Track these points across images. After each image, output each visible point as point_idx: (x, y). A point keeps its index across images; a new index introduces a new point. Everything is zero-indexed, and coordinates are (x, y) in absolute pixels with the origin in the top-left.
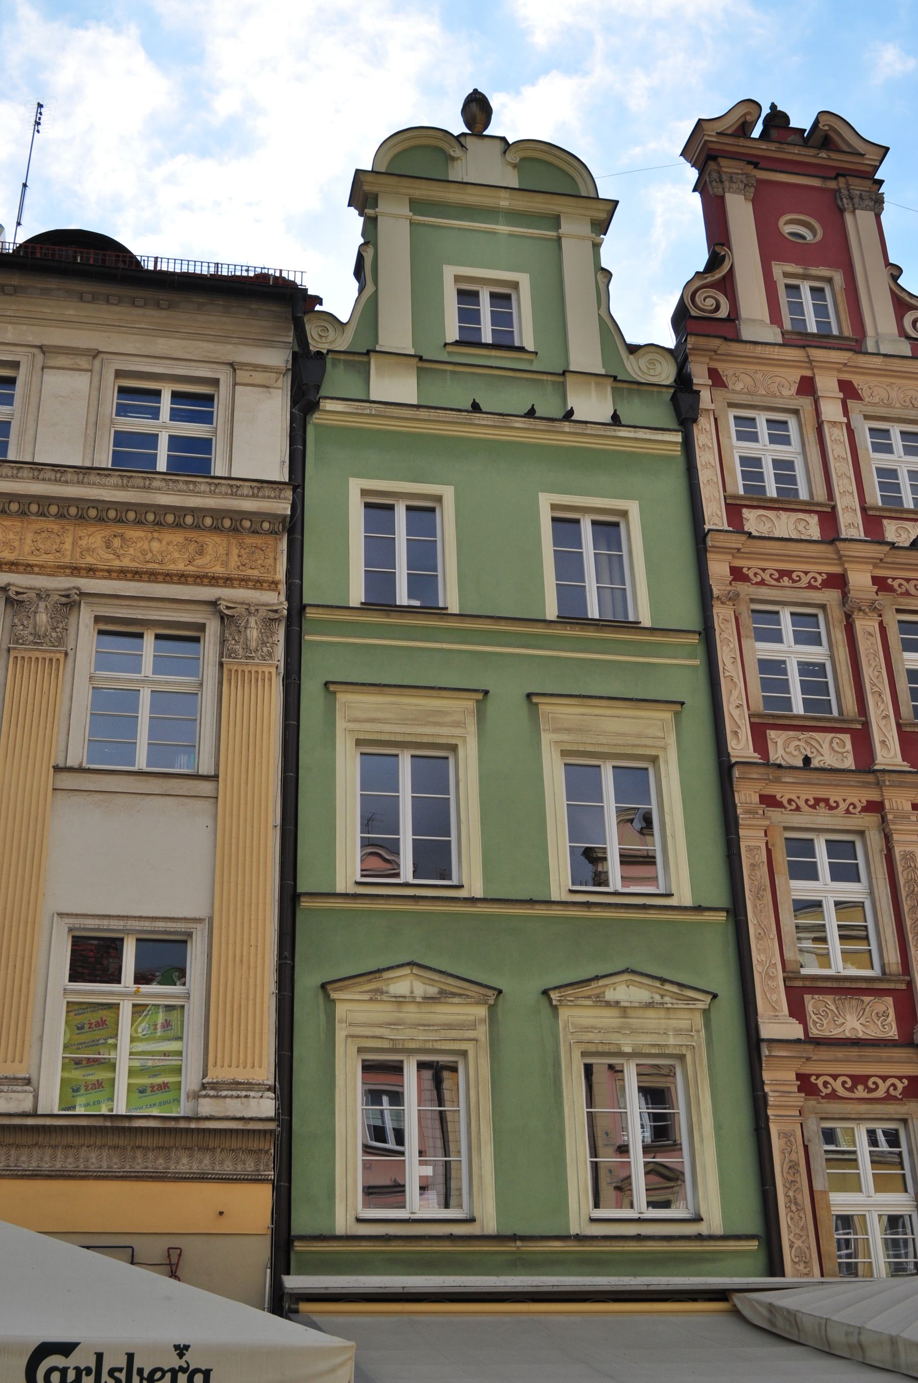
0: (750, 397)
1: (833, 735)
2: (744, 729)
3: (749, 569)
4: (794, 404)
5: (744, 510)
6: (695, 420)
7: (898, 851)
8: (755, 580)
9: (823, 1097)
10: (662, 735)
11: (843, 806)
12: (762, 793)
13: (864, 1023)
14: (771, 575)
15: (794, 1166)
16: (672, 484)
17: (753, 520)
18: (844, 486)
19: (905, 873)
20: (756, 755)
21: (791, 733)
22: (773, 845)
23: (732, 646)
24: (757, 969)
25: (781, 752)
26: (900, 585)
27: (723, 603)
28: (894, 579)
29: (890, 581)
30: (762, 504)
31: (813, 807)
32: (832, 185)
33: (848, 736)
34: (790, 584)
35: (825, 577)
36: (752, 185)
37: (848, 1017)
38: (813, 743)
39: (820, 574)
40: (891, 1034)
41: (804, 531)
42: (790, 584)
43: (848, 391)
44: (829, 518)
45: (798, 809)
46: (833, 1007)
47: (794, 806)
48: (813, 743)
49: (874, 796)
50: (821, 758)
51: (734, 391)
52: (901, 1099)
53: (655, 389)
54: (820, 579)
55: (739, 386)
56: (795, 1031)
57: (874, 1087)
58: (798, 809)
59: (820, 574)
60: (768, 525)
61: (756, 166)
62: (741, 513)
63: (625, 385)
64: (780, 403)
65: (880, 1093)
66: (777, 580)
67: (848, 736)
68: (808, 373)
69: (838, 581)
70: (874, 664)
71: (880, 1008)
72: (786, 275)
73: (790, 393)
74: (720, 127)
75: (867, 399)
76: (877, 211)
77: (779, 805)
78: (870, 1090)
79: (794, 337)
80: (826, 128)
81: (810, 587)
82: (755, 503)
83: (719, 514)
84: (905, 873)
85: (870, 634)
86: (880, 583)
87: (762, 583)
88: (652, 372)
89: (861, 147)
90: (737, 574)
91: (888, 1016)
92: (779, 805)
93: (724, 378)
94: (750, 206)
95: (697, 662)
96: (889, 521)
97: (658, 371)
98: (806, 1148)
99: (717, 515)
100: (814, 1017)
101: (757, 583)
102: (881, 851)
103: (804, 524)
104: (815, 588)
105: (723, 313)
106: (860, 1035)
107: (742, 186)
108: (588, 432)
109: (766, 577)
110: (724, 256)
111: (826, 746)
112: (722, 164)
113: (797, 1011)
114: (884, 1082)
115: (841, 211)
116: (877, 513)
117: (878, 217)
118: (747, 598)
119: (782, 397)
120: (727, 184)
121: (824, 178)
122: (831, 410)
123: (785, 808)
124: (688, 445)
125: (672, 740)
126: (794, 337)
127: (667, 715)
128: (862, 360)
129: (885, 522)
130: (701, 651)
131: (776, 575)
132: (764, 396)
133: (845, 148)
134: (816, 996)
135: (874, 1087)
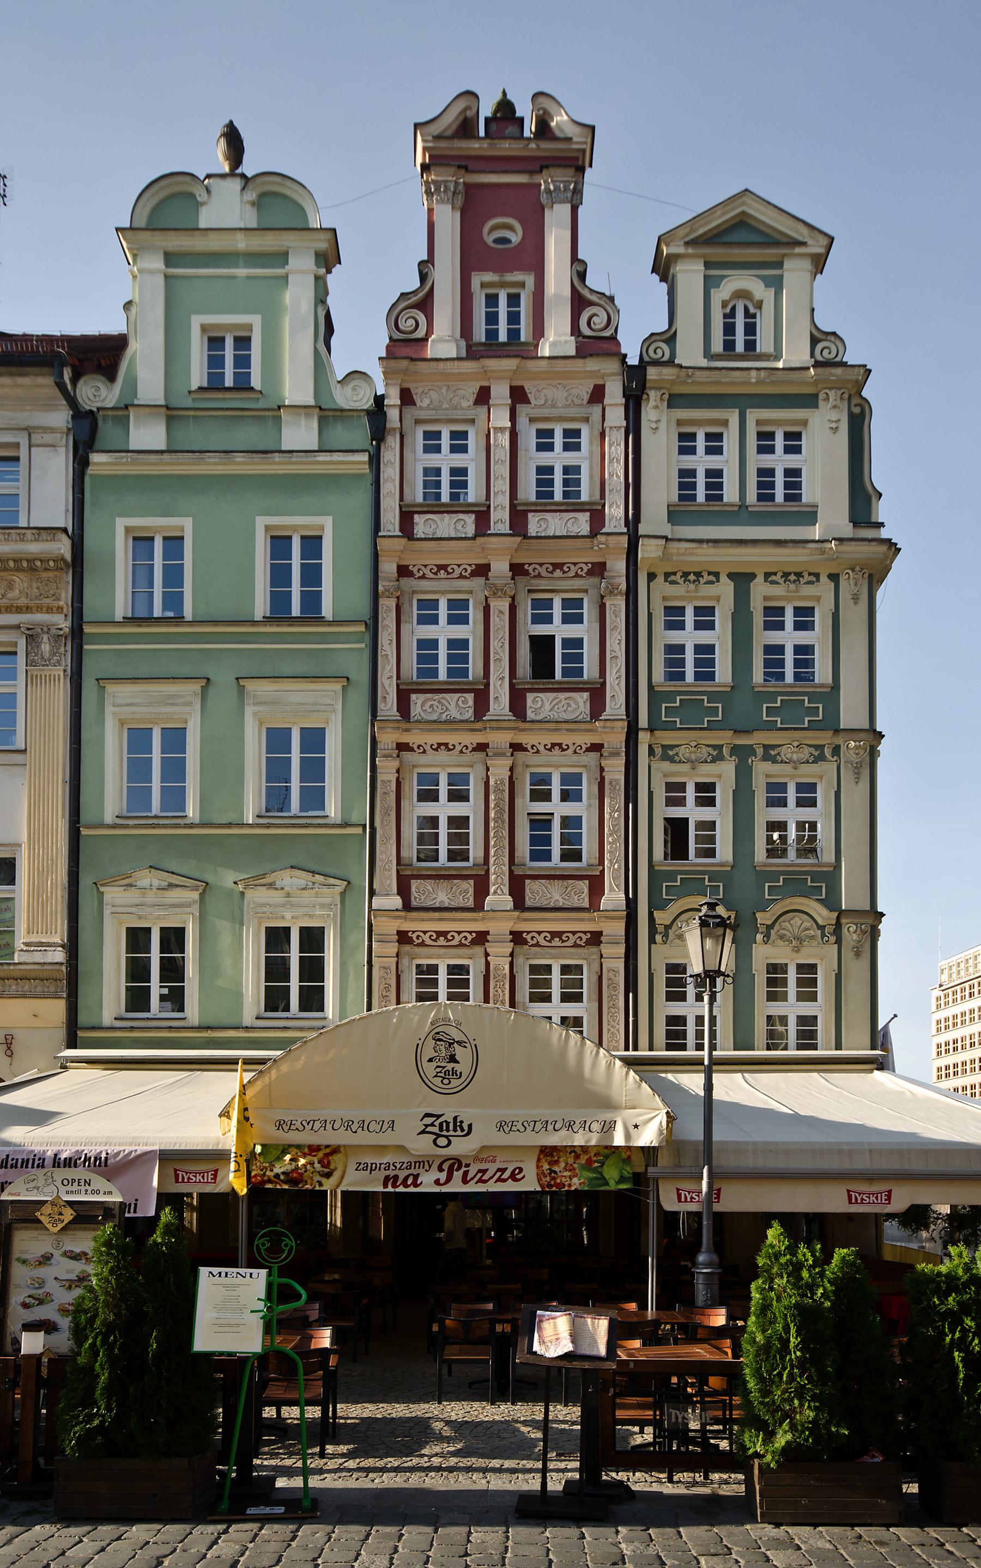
4: (470, 414)
5: (416, 516)
11: (458, 748)
16: (361, 499)
17: (422, 525)
18: (501, 485)
21: (429, 695)
30: (431, 509)
34: (445, 576)
35: (474, 567)
39: (470, 565)
42: (445, 576)
43: (518, 395)
44: (483, 516)
45: (424, 752)
47: (422, 750)
48: (444, 701)
51: (421, 408)
53: (355, 414)
55: (426, 402)
59: (470, 565)
62: (413, 519)
63: (331, 413)
64: (459, 414)
66: (435, 574)
68: (485, 384)
69: (482, 570)
72: (483, 285)
75: (533, 402)
77: (412, 750)
79: (480, 348)
81: (461, 577)
82: (425, 509)
85: (501, 612)
86: (517, 570)
87: (423, 577)
88: (355, 398)
90: (404, 571)
92: (412, 750)
95: (364, 645)
97: (359, 397)
104: (465, 577)
105: (421, 333)
108: (294, 459)
109: (427, 571)
111: (453, 703)
116: (525, 508)
119: (462, 409)
122: (500, 418)
126: (480, 348)
127: (337, 687)
130: (367, 638)
131: (435, 569)
132: (447, 409)
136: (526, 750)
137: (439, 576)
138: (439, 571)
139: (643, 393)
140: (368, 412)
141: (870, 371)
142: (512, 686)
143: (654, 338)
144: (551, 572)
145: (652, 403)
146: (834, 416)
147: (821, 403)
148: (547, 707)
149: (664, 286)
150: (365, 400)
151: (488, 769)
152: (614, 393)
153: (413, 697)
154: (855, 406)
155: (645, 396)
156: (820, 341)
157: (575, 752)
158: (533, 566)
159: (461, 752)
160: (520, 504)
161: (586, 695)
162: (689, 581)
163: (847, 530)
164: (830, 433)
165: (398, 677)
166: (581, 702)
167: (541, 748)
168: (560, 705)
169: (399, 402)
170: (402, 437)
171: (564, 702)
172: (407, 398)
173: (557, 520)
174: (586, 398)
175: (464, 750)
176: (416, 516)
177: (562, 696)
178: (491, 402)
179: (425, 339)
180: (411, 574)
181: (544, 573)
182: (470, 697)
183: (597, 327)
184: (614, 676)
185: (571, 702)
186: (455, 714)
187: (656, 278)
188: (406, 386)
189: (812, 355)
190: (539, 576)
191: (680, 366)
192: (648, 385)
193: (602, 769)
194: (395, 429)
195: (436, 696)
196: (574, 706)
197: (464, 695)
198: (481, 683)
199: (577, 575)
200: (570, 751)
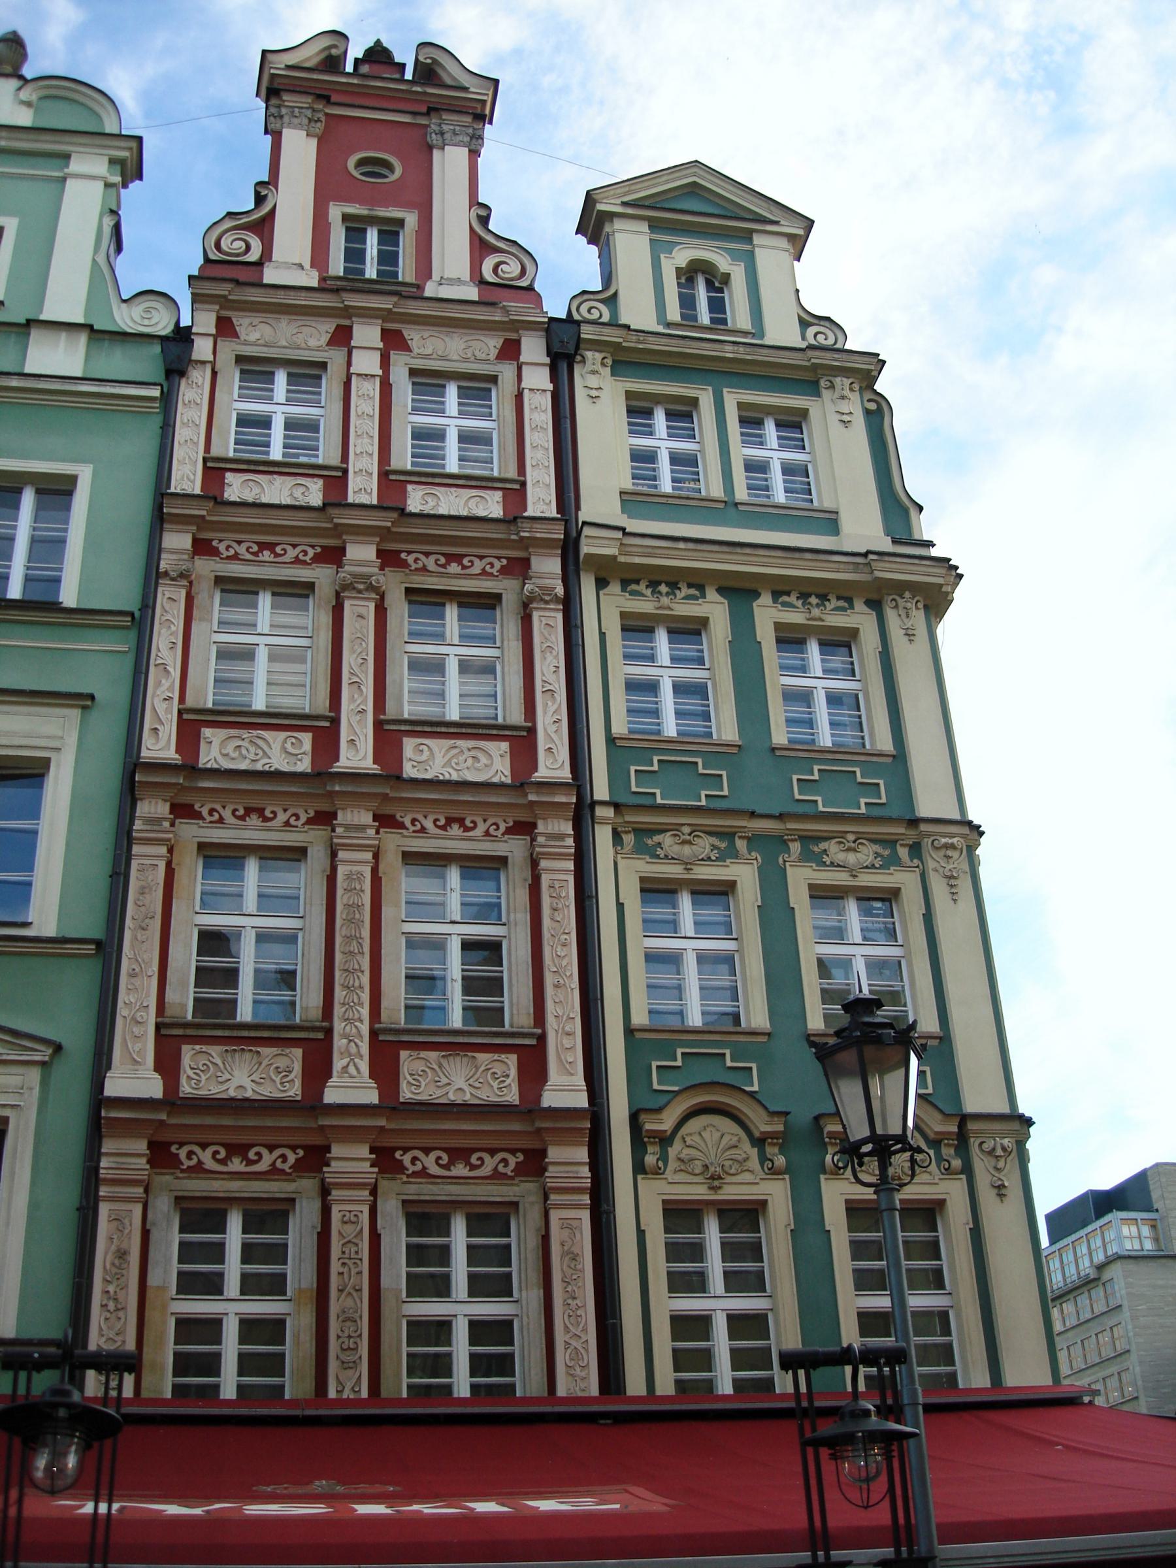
0: (265, 349)
1: (289, 734)
2: (167, 727)
3: (221, 541)
4: (319, 357)
5: (228, 475)
6: (182, 374)
7: (341, 870)
8: (225, 554)
9: (183, 1171)
10: (60, 734)
11: (282, 817)
12: (176, 801)
13: (257, 1080)
14: (247, 550)
15: (122, 1254)
17: (236, 488)
18: (365, 445)
19: (346, 897)
20: (177, 756)
21: (233, 732)
22: (178, 864)
23: (173, 628)
24: (122, 1011)
25: (215, 752)
26: (416, 560)
27: (173, 579)
28: (409, 553)
29: (403, 555)
31: (242, 818)
32: (423, 121)
33: (310, 735)
34: (272, 559)
36: (319, 120)
37: (236, 1073)
38: (260, 742)
40: (291, 1093)
41: (301, 498)
42: (272, 559)
46: (219, 1061)
47: (216, 816)
48: (260, 742)
49: (325, 807)
50: (267, 761)
51: (246, 343)
52: (290, 1174)
54: (311, 552)
55: (254, 336)
56: (153, 1087)
57: (256, 1158)
58: (221, 820)
59: (313, 547)
60: (256, 490)
61: (327, 99)
62: (224, 478)
65: (263, 1166)
66: (255, 554)
67: (310, 735)
70: (359, 650)
71: (282, 1062)
73: (319, 343)
74: (291, 59)
75: (416, 351)
76: (473, 147)
78: (250, 1163)
80: (429, 61)
81: (297, 561)
83: (192, 477)
84: (346, 897)
85: (361, 616)
87: (236, 557)
88: (146, 322)
89: (465, 80)
91: (290, 1072)
92: (198, 816)
93: (237, 328)
94: (314, 143)
96: (415, 486)
97: (153, 322)
98: (146, 1234)
99: (189, 479)
100: (190, 1073)
101: (228, 558)
102: (324, 871)
103: (302, 489)
104: (304, 563)
105: (254, 256)
106: (249, 1094)
107: (306, 121)
109: (241, 550)
110: (266, 196)
111: (276, 747)
112: (285, 98)
113: (167, 1064)
114: (271, 1152)
115: (430, 148)
117: (474, 154)
118: (213, 574)
120: (286, 119)
121: (415, 114)
123: (204, 819)
124: (168, 402)
125: (72, 740)
127: (75, 714)
128: (413, 308)
129: (410, 487)
133: (449, 82)
134: (197, 1047)
135: (256, 1158)
136: (402, 826)
137: (261, 558)
138: (261, 550)
139: (576, 354)
140: (163, 339)
141: (884, 362)
142: (378, 725)
143: (586, 297)
144: (444, 566)
145: (589, 366)
146: (844, 407)
147: (824, 392)
148: (439, 760)
149: (594, 249)
150: (160, 326)
151: (334, 855)
152: (533, 349)
153: (207, 732)
154: (869, 401)
155: (578, 358)
156: (810, 325)
157: (487, 833)
158: (414, 556)
159: (287, 823)
160: (396, 472)
161: (505, 746)
162: (660, 593)
163: (886, 545)
164: (841, 425)
165: (182, 699)
166: (495, 754)
167: (429, 824)
168: (461, 758)
169: (214, 332)
170: (214, 374)
171: (467, 754)
172: (225, 328)
173: (452, 498)
174: (494, 353)
175: (292, 821)
176: (228, 475)
177: (463, 744)
178: (353, 343)
179: (259, 264)
180: (215, 552)
181: (431, 565)
182: (307, 739)
183: (507, 276)
184: (549, 719)
185: (480, 755)
186: (279, 763)
187: (582, 240)
188: (225, 313)
189: (804, 338)
190: (424, 569)
191: (627, 327)
192: (582, 346)
193: (534, 864)
194: (203, 363)
195: (245, 734)
196: (484, 760)
197: (295, 734)
198: (325, 718)
199: (484, 572)
200: (479, 832)
